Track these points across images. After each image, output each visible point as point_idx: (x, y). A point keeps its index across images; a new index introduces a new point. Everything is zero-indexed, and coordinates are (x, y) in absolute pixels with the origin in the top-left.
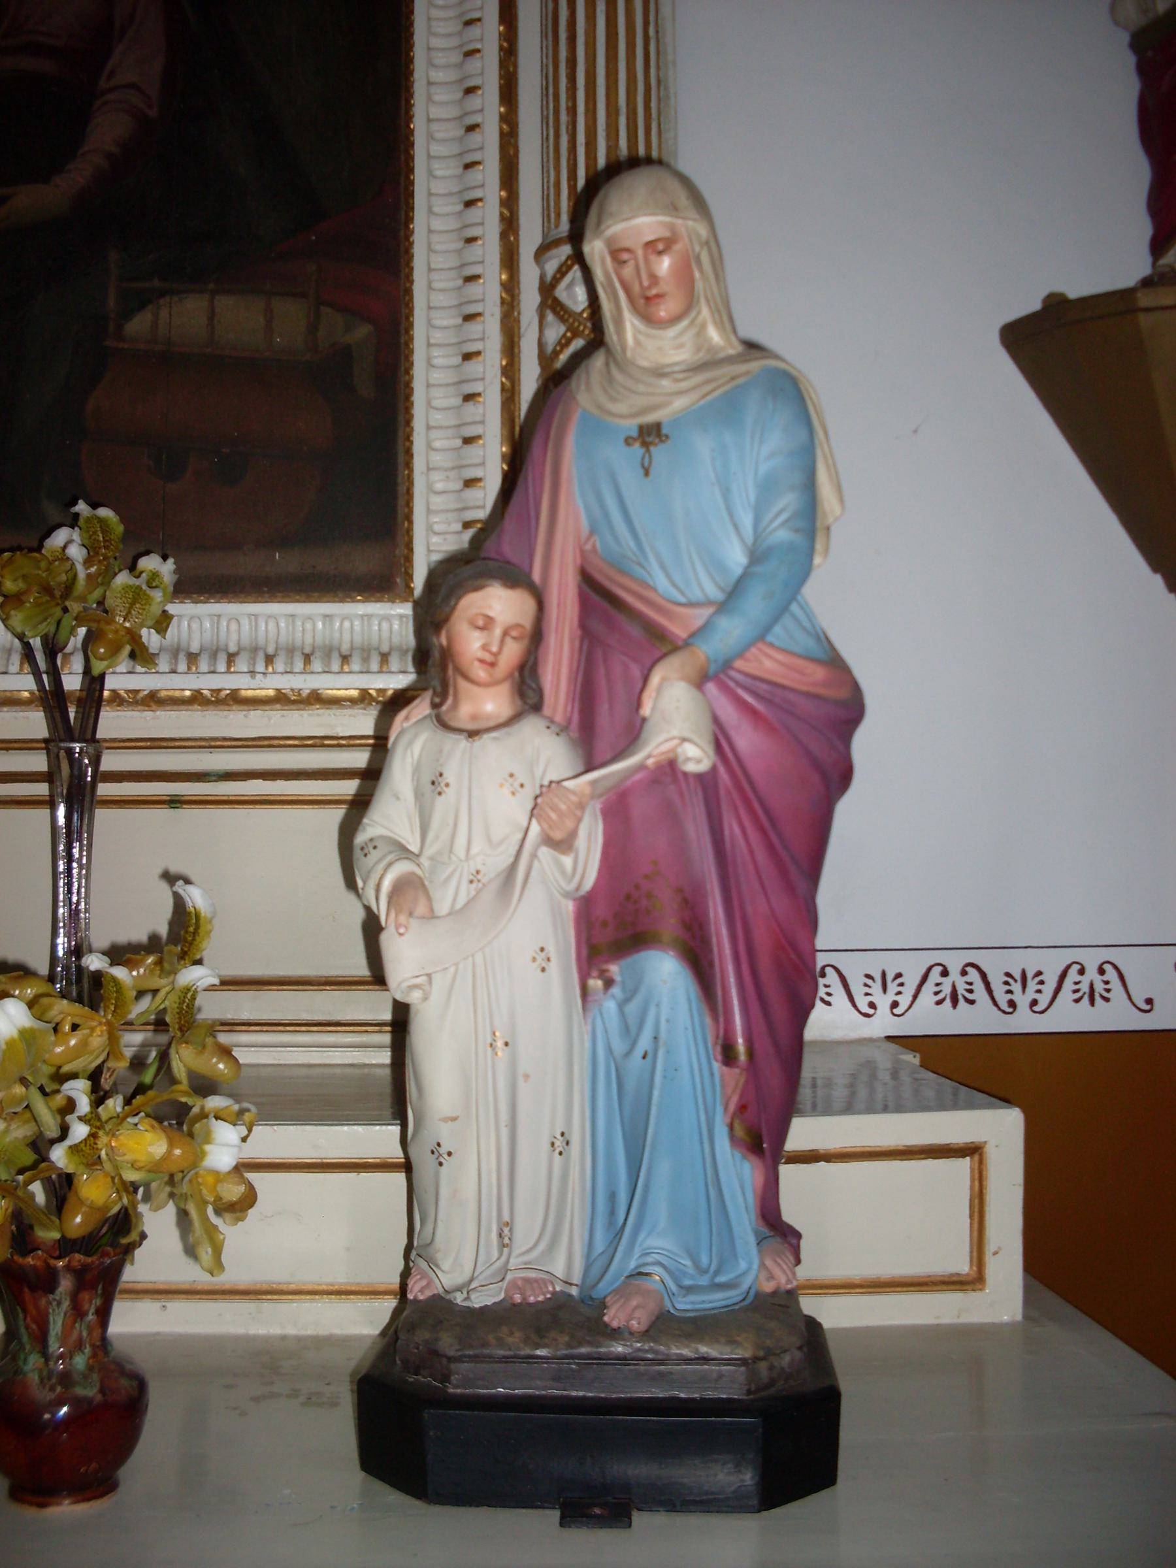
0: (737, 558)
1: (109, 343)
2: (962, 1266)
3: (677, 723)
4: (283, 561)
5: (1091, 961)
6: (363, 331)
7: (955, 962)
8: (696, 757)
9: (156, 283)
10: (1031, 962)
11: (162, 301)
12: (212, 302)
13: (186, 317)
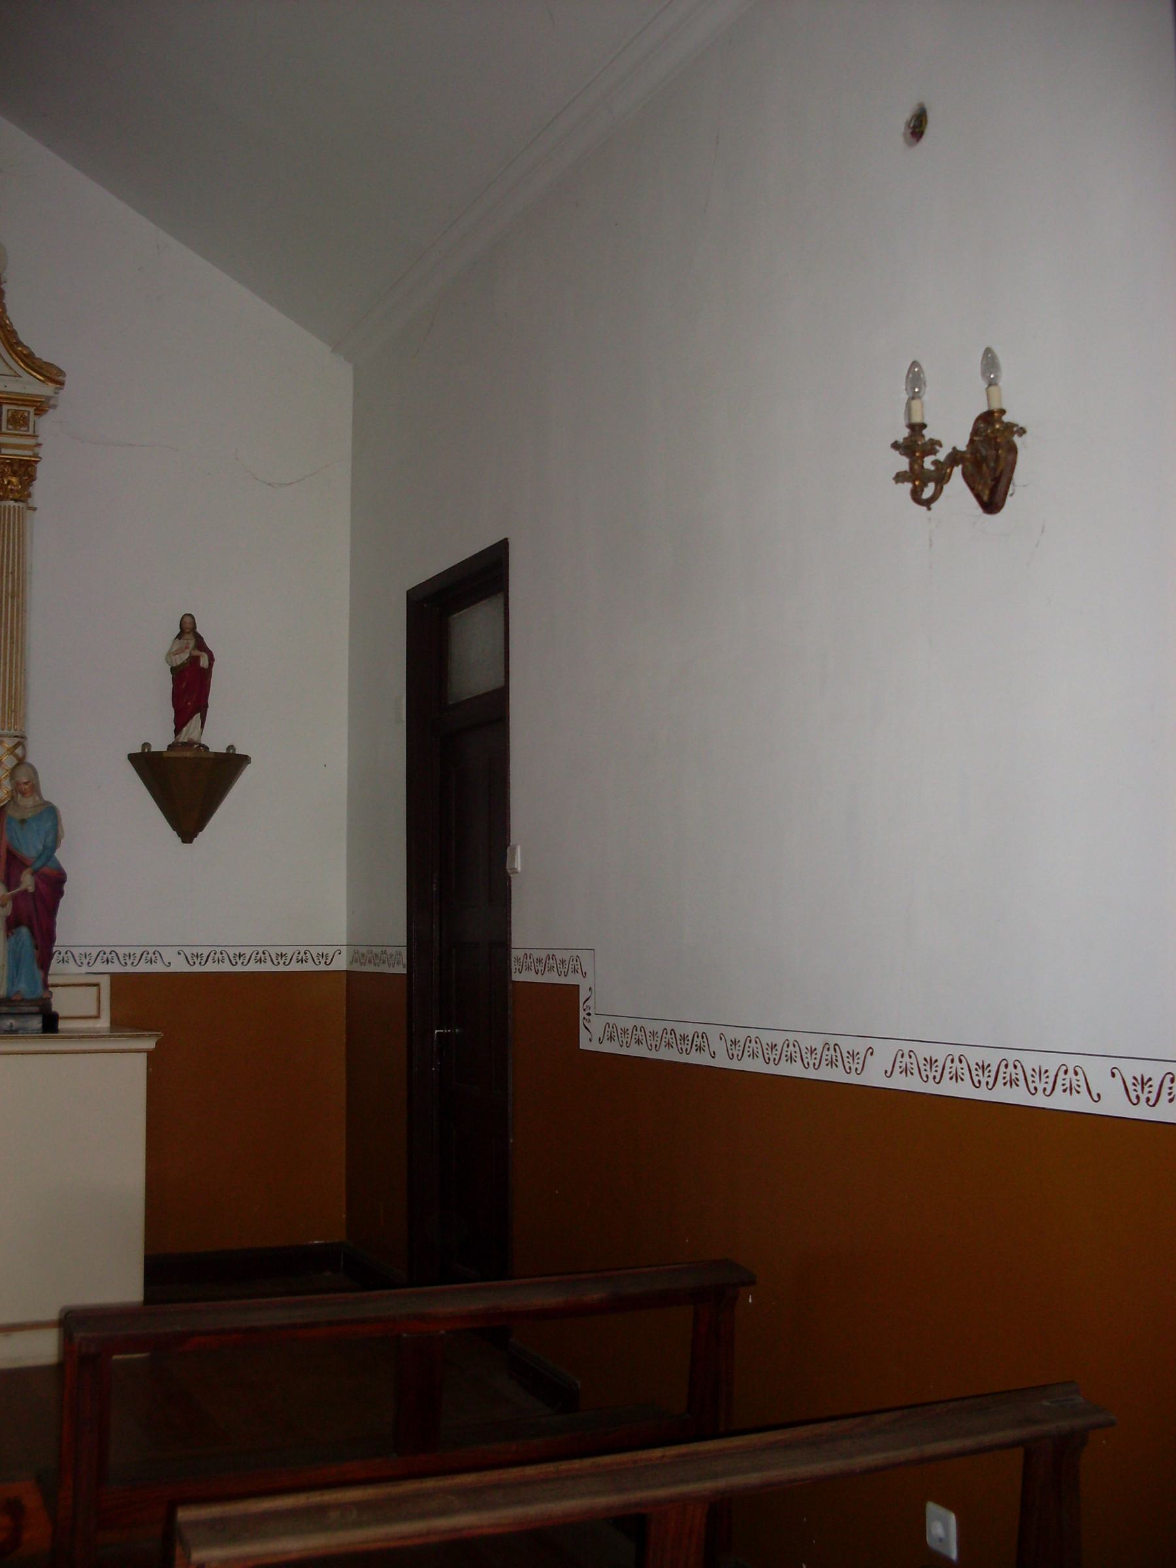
0: (40, 847)
2: (94, 1013)
3: (27, 881)
5: (151, 950)
7: (108, 950)
8: (31, 889)
10: (132, 950)
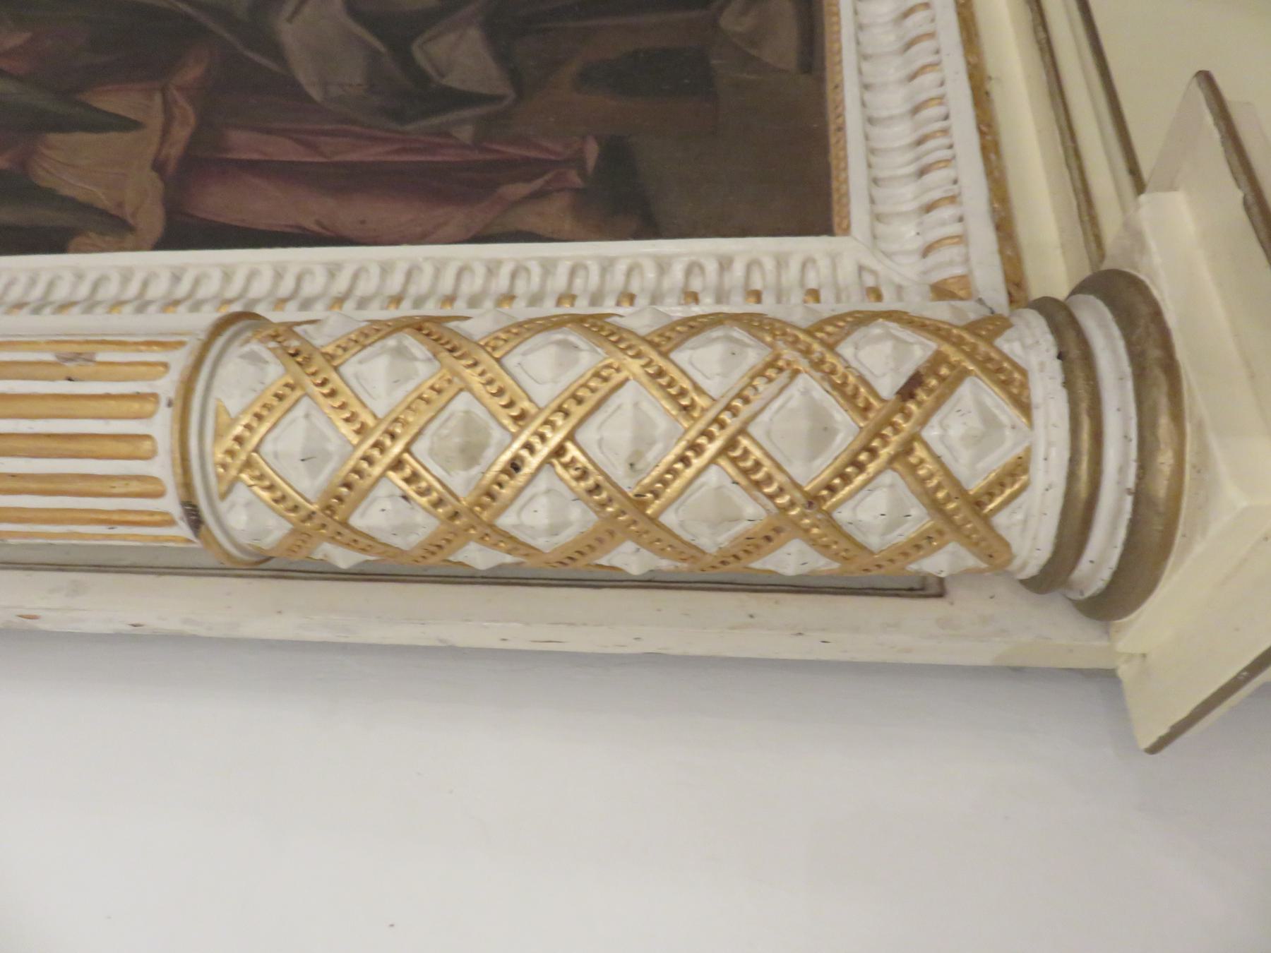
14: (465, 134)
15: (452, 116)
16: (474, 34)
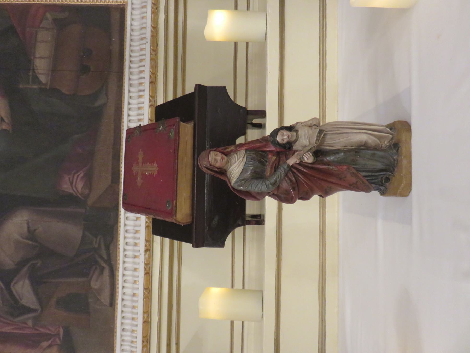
1: (48, 87)
4: (115, 39)
6: (48, 15)
9: (30, 73)
11: (36, 71)
12: (37, 58)
13: (41, 65)
14: (30, 323)
15: (26, 316)
16: (27, 282)
